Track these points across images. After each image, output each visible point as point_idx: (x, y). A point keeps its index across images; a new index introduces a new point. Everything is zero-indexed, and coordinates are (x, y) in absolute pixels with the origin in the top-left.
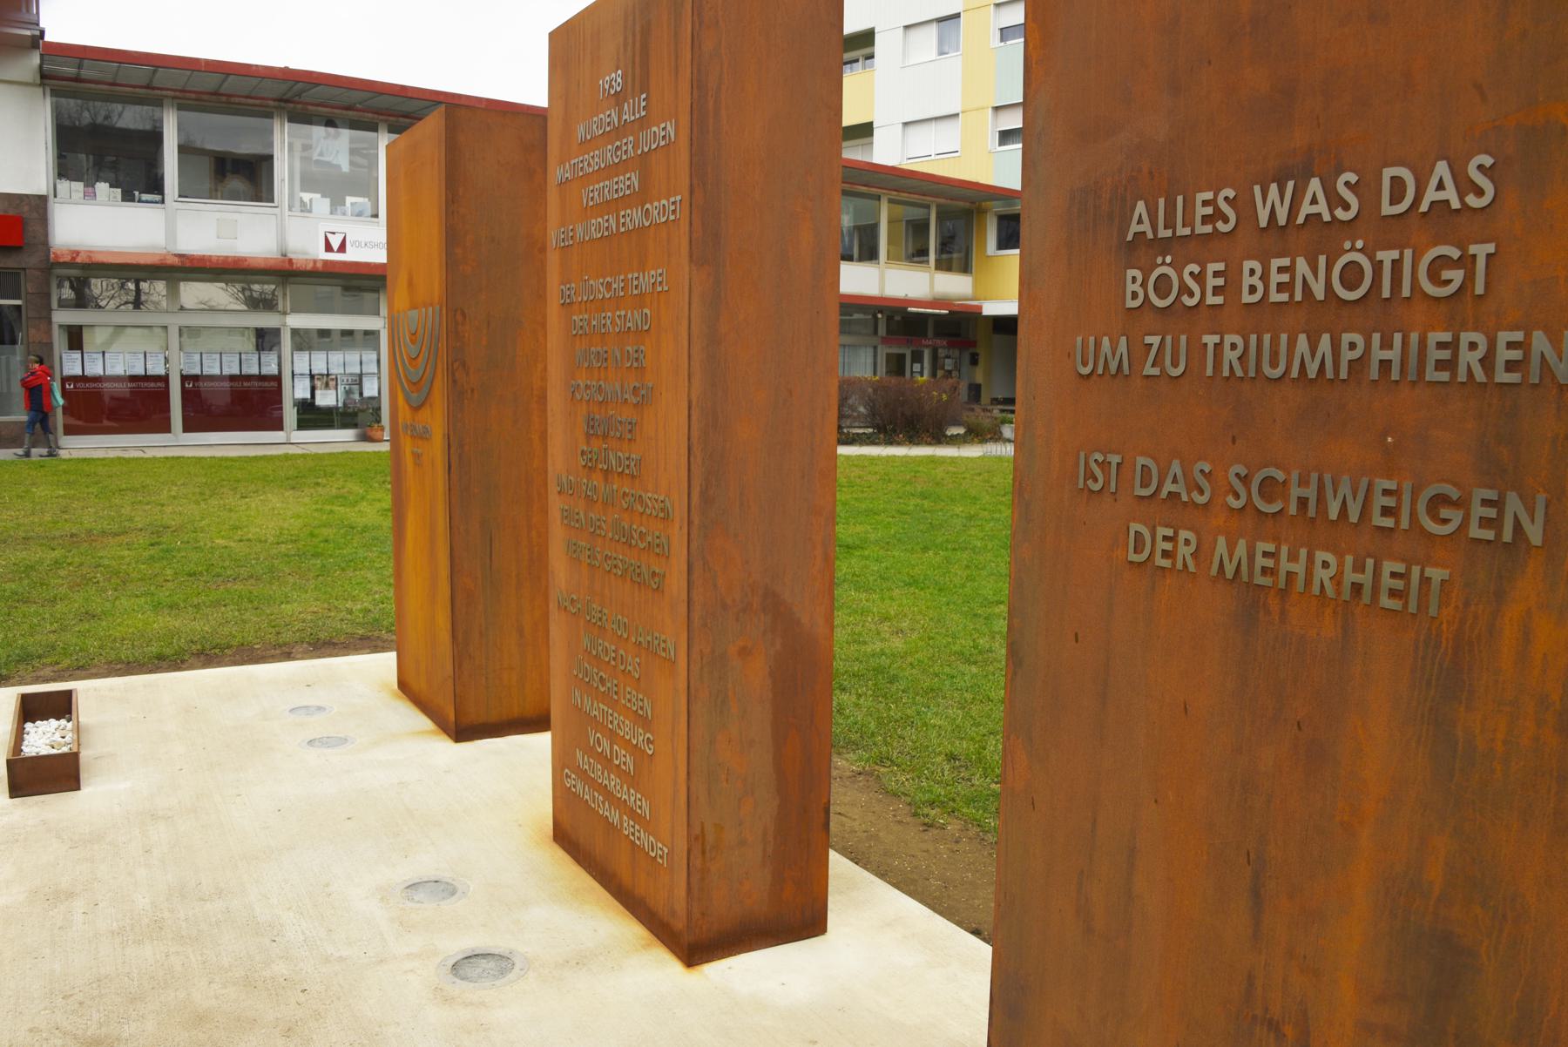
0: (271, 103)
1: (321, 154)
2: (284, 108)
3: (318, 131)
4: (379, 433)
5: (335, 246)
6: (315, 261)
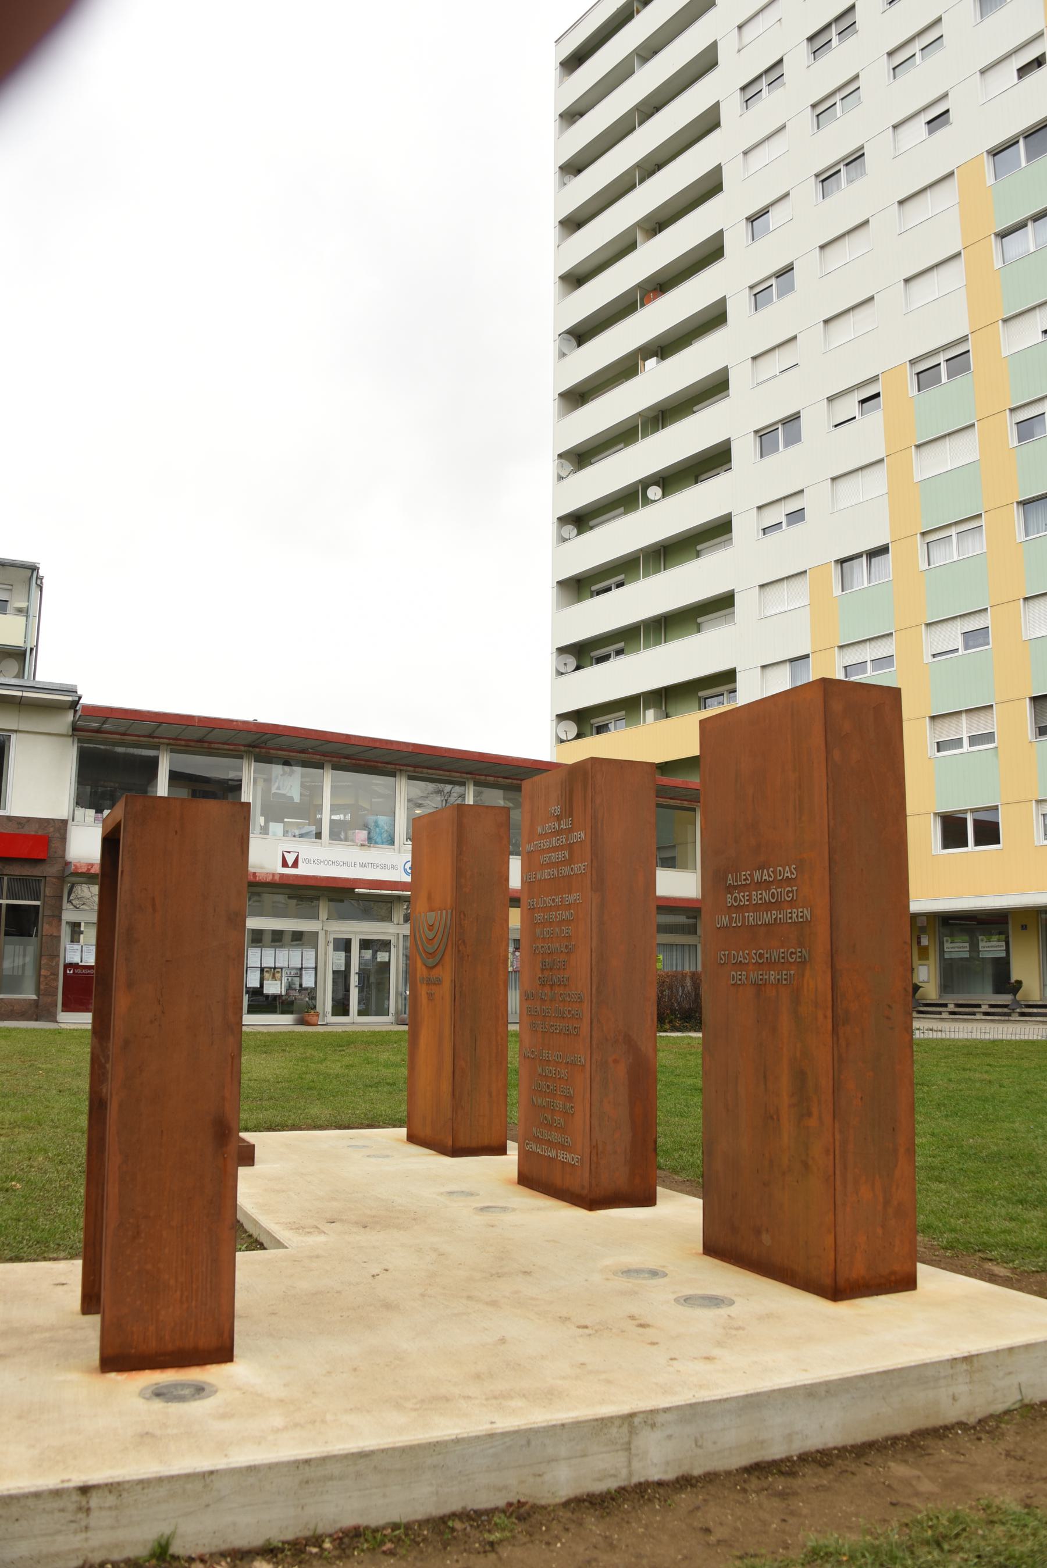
0: (242, 748)
1: (278, 788)
2: (252, 752)
3: (277, 769)
4: (315, 1018)
5: (290, 862)
6: (274, 875)
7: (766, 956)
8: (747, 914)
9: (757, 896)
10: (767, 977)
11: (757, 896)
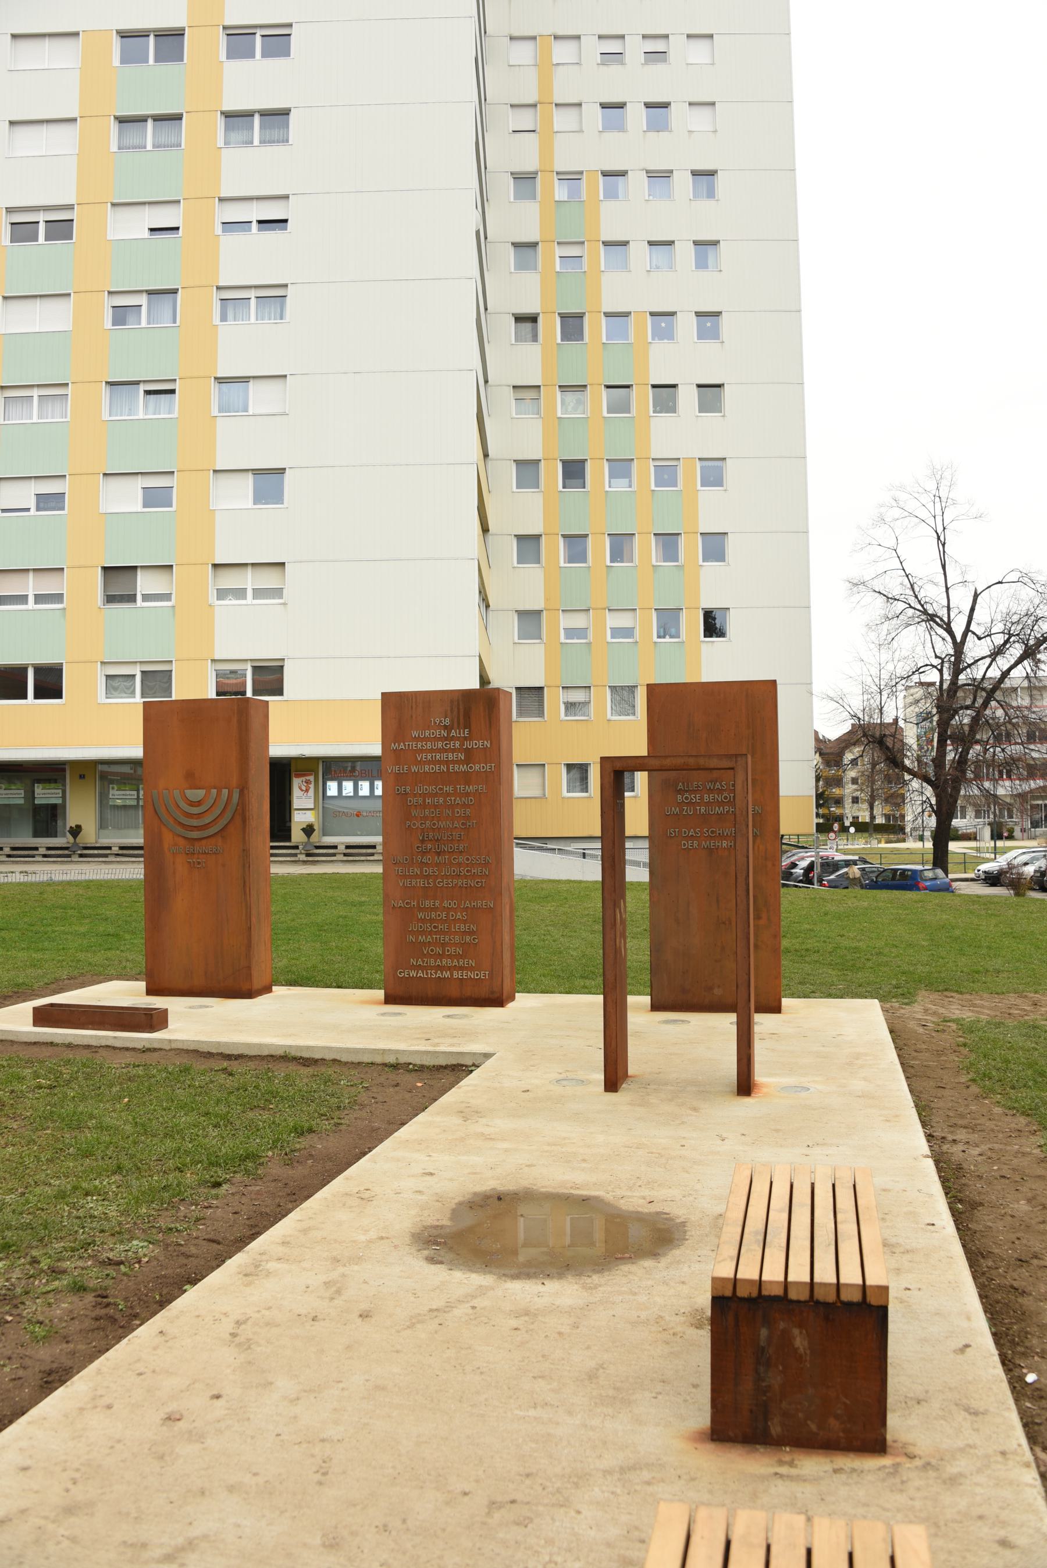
7: (718, 832)
8: (698, 808)
9: (709, 798)
10: (720, 844)
11: (709, 798)
